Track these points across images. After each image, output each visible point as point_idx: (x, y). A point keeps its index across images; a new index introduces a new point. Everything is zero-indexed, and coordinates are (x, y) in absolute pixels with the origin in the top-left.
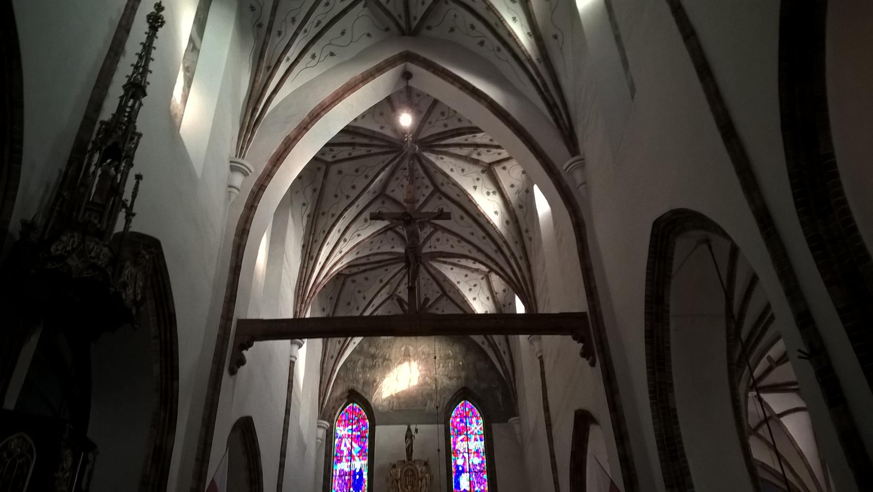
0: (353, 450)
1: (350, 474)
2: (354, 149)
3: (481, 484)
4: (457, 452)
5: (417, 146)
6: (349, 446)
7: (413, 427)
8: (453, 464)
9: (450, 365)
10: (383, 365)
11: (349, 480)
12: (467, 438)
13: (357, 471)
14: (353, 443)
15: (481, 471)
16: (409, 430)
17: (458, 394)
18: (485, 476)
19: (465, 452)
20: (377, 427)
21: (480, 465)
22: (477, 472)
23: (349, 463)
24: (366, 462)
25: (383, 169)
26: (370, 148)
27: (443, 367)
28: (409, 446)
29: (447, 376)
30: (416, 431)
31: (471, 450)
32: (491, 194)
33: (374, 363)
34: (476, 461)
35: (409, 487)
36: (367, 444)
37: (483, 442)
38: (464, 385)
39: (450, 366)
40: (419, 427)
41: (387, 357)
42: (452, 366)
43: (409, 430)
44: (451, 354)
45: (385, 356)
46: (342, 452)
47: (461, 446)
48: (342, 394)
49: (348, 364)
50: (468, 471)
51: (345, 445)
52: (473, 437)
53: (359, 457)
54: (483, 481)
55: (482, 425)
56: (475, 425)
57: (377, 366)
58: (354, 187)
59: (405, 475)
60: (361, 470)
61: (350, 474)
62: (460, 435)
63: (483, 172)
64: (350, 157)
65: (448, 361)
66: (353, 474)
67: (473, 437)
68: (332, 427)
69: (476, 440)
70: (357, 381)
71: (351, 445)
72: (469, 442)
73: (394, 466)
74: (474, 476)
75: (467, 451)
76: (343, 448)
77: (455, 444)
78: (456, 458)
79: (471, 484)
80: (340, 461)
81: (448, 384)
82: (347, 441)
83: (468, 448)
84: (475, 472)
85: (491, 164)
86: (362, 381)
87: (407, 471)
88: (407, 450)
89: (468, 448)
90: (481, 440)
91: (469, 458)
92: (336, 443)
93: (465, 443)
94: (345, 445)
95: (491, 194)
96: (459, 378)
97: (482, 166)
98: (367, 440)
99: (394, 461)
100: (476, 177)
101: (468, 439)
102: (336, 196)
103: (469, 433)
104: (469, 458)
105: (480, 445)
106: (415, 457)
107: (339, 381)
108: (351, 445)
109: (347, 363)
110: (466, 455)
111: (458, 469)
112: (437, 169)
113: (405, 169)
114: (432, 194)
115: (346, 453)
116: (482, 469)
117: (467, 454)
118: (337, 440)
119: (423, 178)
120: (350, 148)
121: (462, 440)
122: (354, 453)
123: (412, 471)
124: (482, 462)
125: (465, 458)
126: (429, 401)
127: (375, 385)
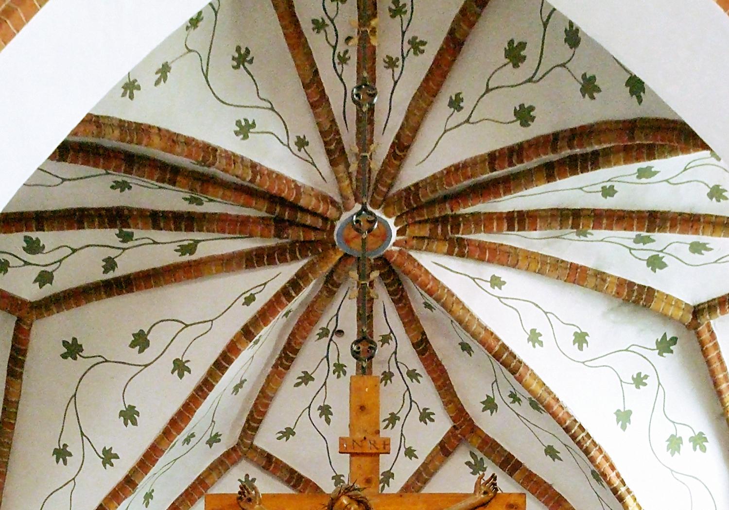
2: (126, 238)
5: (391, 221)
25: (248, 333)
26: (195, 235)
32: (687, 446)
58: (129, 415)
63: (665, 346)
64: (111, 275)
85: (697, 311)
95: (687, 446)
97: (665, 317)
100: (632, 365)
102: (62, 454)
112: (474, 335)
113: (340, 333)
114: (445, 449)
119: (413, 375)
120: (109, 235)
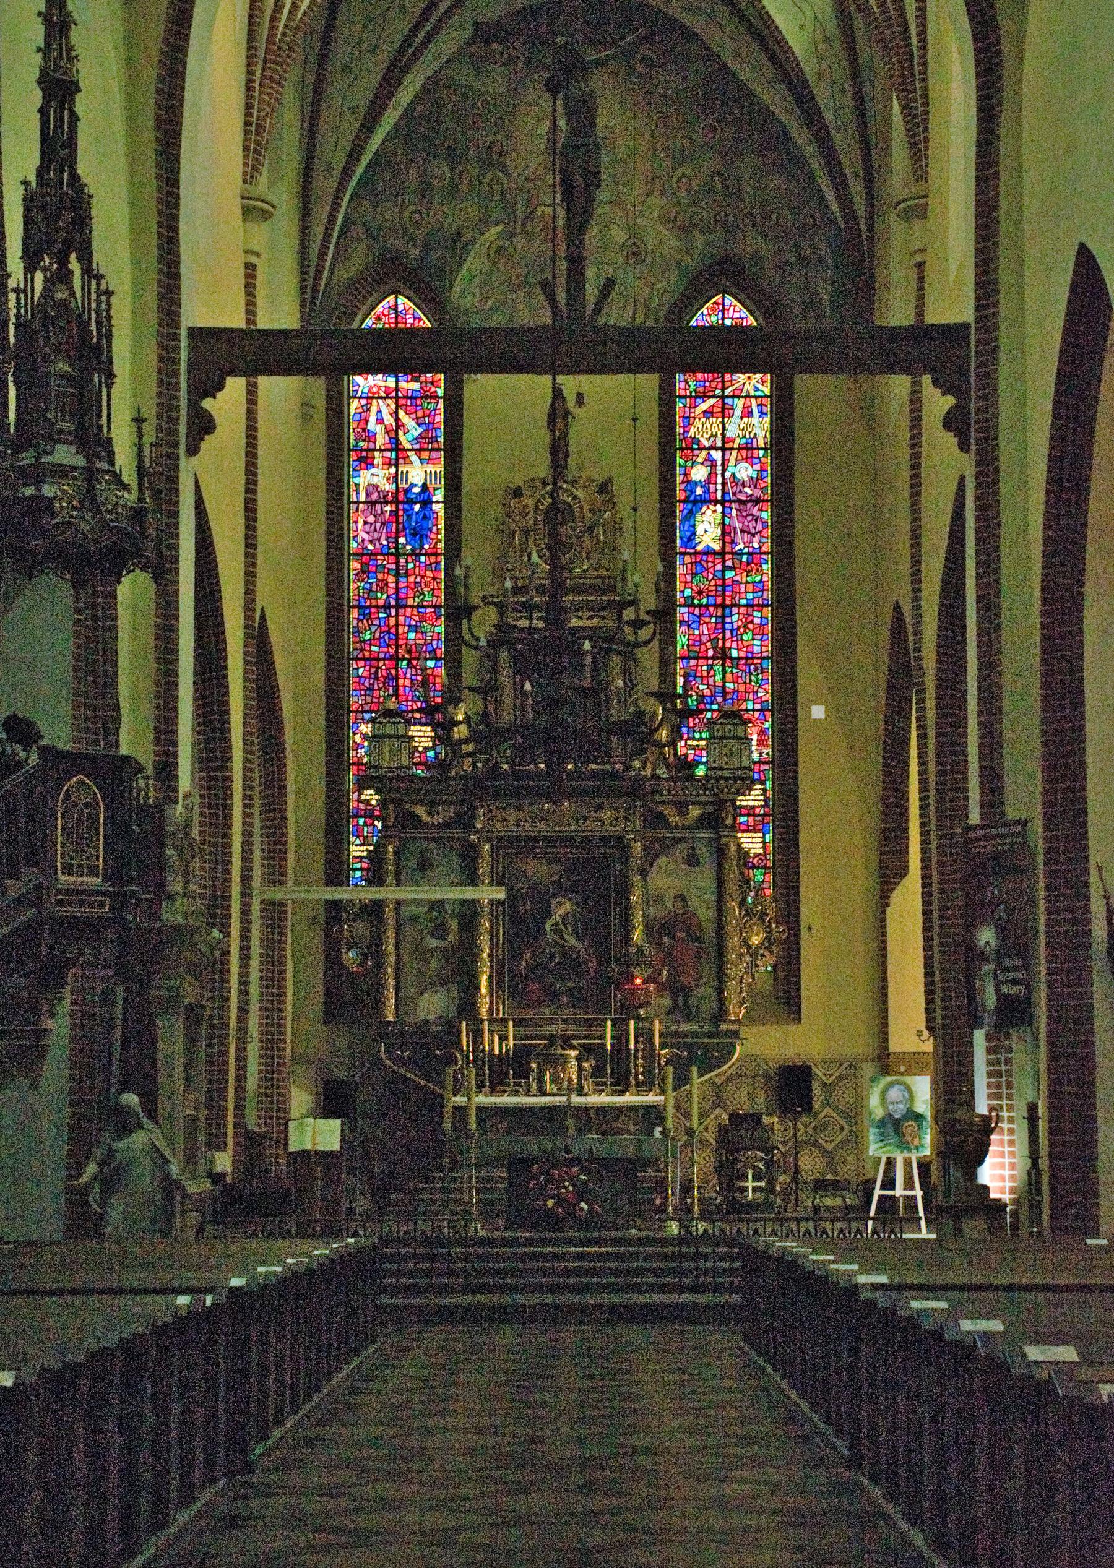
0: (401, 433)
1: (396, 501)
3: (753, 535)
4: (692, 446)
6: (389, 420)
8: (679, 479)
11: (395, 514)
13: (416, 490)
14: (401, 413)
15: (757, 501)
18: (766, 515)
21: (754, 482)
23: (393, 470)
24: (439, 468)
31: (733, 441)
34: (744, 472)
36: (440, 419)
37: (767, 419)
46: (371, 437)
47: (703, 430)
50: (719, 496)
51: (380, 421)
52: (739, 403)
53: (418, 451)
54: (759, 527)
60: (425, 487)
61: (396, 501)
62: (704, 397)
66: (401, 498)
69: (747, 413)
71: (397, 420)
74: (734, 513)
75: (719, 444)
76: (372, 426)
77: (688, 421)
78: (689, 463)
79: (726, 532)
80: (366, 462)
82: (386, 408)
84: (740, 501)
89: (723, 435)
90: (762, 414)
92: (352, 412)
93: (716, 421)
94: (380, 421)
98: (441, 405)
101: (725, 411)
103: (727, 392)
105: (760, 428)
108: (397, 420)
110: (717, 455)
111: (693, 492)
115: (381, 440)
116: (758, 493)
117: (720, 453)
118: (355, 404)
121: (708, 413)
122: (405, 441)
124: (760, 478)
125: (713, 465)
127: (459, 246)
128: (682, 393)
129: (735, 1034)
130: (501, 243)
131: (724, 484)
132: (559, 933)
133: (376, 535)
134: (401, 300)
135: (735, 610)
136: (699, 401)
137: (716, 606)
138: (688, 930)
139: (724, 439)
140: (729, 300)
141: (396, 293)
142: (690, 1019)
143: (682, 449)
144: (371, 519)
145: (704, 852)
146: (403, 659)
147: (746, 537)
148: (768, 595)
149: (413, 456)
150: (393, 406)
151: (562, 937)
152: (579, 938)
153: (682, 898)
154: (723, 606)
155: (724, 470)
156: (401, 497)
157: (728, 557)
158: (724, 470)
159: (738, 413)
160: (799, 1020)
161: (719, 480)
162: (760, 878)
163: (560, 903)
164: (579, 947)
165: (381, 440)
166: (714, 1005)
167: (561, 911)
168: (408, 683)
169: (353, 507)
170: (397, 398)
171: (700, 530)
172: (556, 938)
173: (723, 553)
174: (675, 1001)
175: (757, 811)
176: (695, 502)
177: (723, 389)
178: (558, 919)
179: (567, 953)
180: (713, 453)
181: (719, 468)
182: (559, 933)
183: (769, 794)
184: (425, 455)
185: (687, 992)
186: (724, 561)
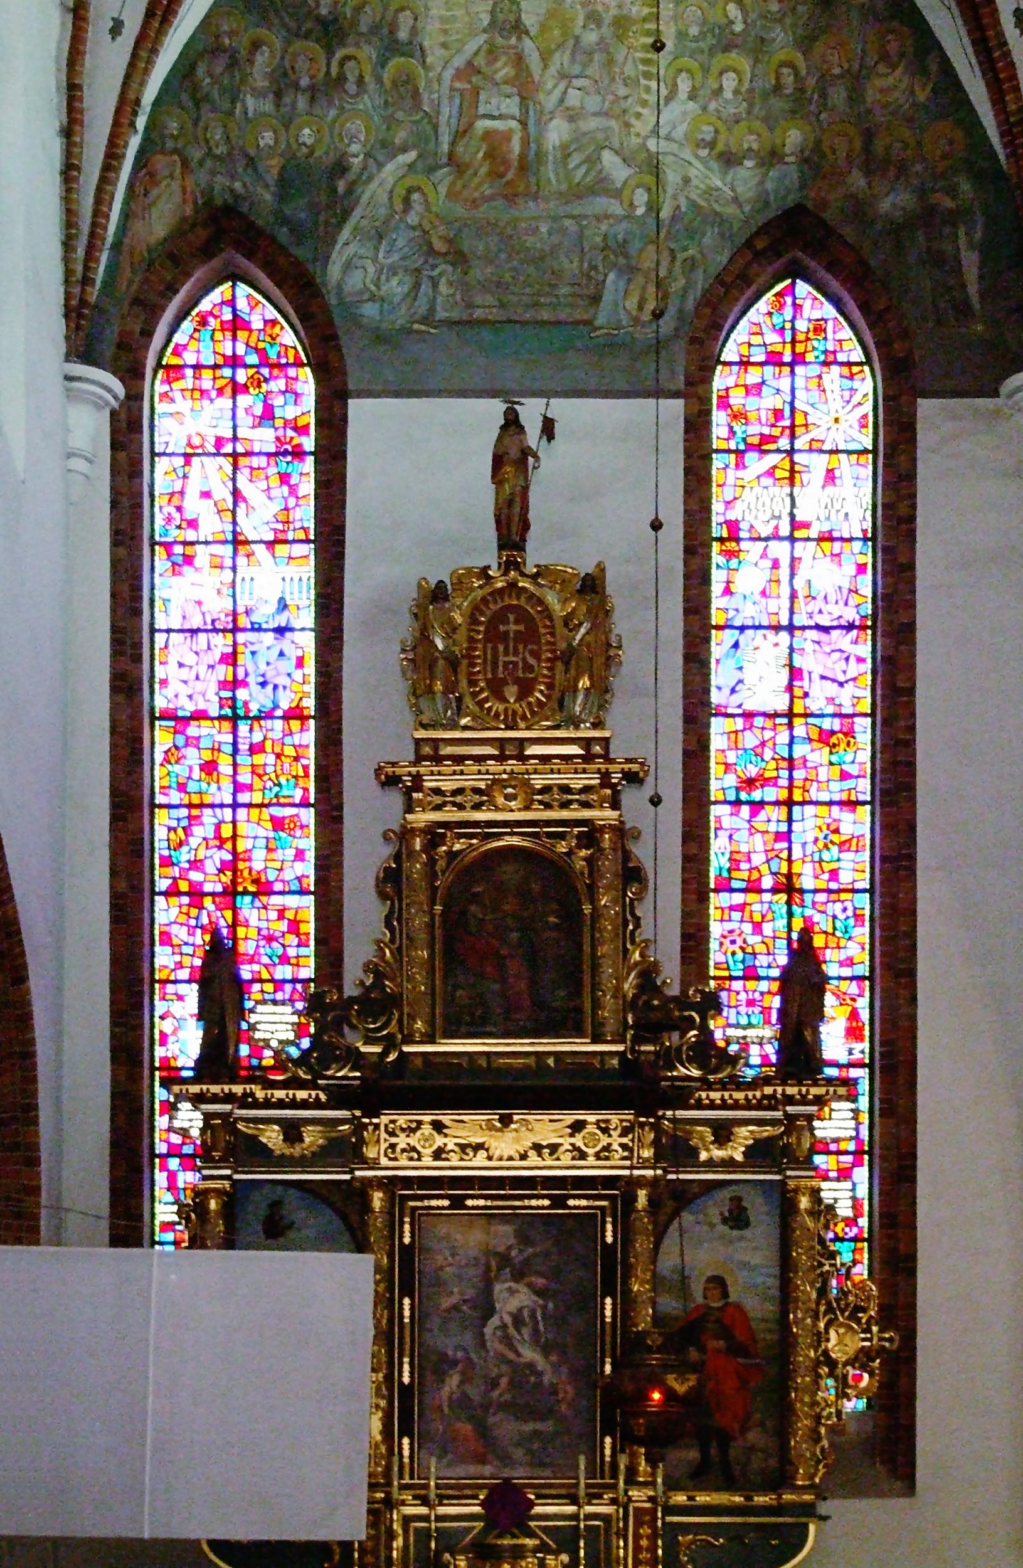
6: (223, 493)
7: (531, 412)
9: (729, 82)
10: (379, 80)
12: (792, 471)
16: (512, 423)
17: (760, 245)
19: (776, 537)
20: (354, 405)
22: (826, 630)
27: (692, 97)
28: (510, 503)
29: (712, 145)
30: (548, 428)
31: (807, 525)
33: (334, 70)
35: (511, 692)
38: (791, 200)
39: (728, 94)
40: (562, 409)
41: (403, 35)
42: (736, 92)
43: (512, 423)
44: (738, 27)
45: (393, 29)
48: (181, 231)
49: (201, 70)
53: (270, 545)
55: (868, 407)
56: (835, 403)
57: (351, 87)
59: (494, 635)
65: (720, 60)
67: (818, 464)
68: (134, 397)
70: (251, 162)
71: (236, 494)
72: (796, 490)
73: (438, 594)
75: (785, 530)
76: (194, 506)
81: (710, 191)
83: (792, 515)
84: (818, 627)
86: (273, 166)
87: (500, 617)
88: (502, 522)
89: (792, 515)
91: (794, 561)
96: (772, 157)
99: (439, 573)
103: (798, 444)
104: (794, 561)
106: (535, 555)
107: (161, 162)
109: (193, 67)
115: (211, 525)
123: (522, 616)
126: (611, 277)
128: (723, 445)
129: (808, 1510)
130: (409, 182)
131: (793, 595)
132: (507, 1340)
133: (199, 686)
134: (243, 290)
135: (809, 810)
136: (751, 457)
137: (777, 803)
138: (726, 1332)
139: (795, 525)
140: (803, 288)
141: (235, 277)
142: (730, 1485)
143: (721, 540)
144: (190, 659)
145: (759, 1209)
146: (245, 892)
147: (831, 689)
148: (865, 785)
149: (260, 550)
150: (229, 469)
151: (511, 1346)
152: (546, 1350)
153: (718, 1283)
154: (789, 803)
155: (792, 575)
156: (243, 621)
157: (797, 721)
158: (792, 575)
159: (819, 475)
160: (908, 1485)
161: (785, 591)
162: (847, 1257)
163: (512, 1292)
164: (541, 1362)
165: (211, 525)
166: (773, 1462)
167: (513, 1304)
168: (253, 933)
169: (160, 639)
170: (235, 456)
171: (748, 675)
172: (501, 1348)
173: (790, 715)
174: (705, 1453)
175: (843, 1146)
176: (742, 629)
177: (793, 437)
178: (508, 1320)
179: (522, 1373)
180: (773, 544)
181: (784, 572)
182: (507, 1340)
183: (865, 1118)
184: (281, 549)
185: (725, 1439)
186: (790, 726)
